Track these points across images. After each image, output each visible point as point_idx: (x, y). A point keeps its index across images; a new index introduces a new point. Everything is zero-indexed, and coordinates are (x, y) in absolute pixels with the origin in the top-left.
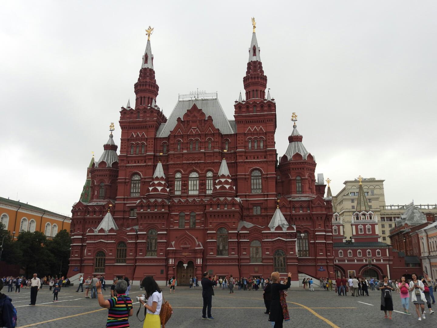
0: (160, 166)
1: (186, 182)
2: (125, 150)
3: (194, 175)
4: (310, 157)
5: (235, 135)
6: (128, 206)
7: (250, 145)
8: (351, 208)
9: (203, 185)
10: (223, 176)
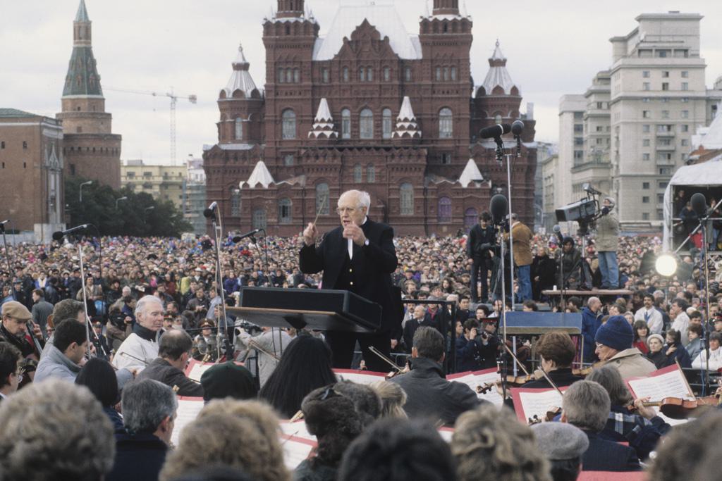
0: (323, 102)
1: (357, 123)
2: (273, 77)
3: (367, 113)
4: (515, 90)
5: (421, 60)
6: (282, 152)
7: (438, 74)
8: (641, 87)
9: (378, 126)
10: (406, 120)
